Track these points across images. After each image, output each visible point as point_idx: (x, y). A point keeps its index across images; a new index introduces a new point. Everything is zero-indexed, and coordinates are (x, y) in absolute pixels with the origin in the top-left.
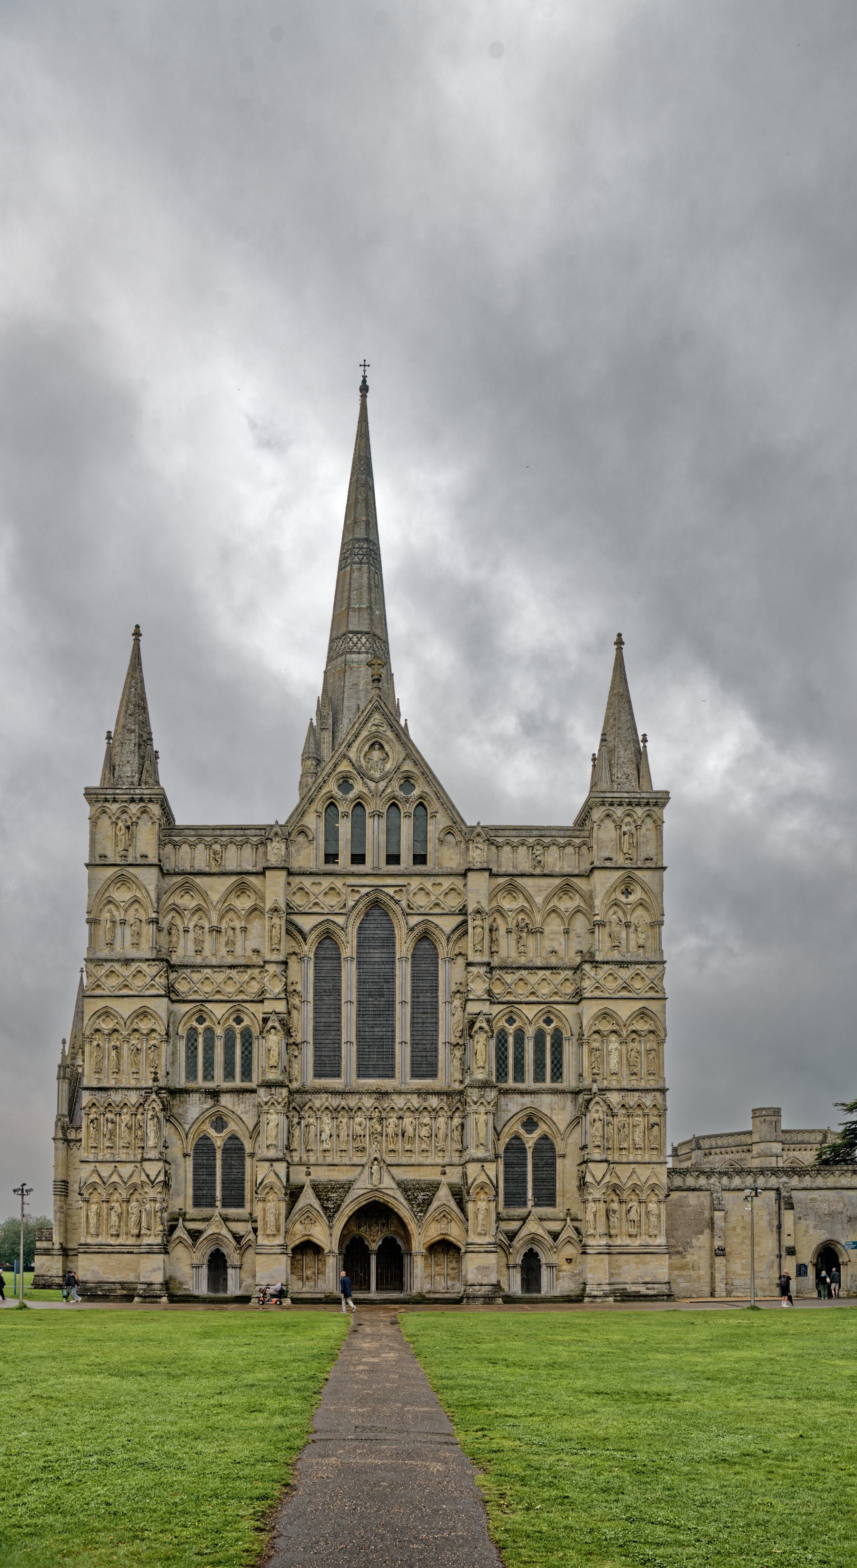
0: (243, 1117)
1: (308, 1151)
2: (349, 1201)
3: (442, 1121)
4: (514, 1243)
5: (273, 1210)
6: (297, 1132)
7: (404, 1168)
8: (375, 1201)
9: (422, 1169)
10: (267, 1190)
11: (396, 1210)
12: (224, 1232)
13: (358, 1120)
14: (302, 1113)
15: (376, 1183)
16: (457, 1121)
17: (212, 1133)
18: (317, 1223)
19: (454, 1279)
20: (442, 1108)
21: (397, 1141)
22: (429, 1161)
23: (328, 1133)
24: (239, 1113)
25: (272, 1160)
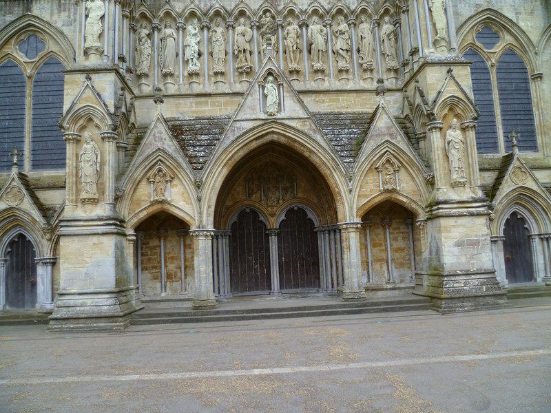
0: (66, 30)
1: (165, 76)
2: (228, 142)
3: (365, 27)
4: (495, 203)
5: (90, 156)
6: (146, 48)
7: (314, 96)
8: (272, 143)
9: (342, 97)
10: (81, 122)
11: (307, 154)
12: (27, 205)
13: (239, 29)
14: (156, 21)
15: (272, 109)
16: (387, 28)
17: (21, 57)
18: (176, 182)
19: (402, 265)
20: (364, 11)
21: (301, 59)
22: (350, 86)
23: (196, 48)
24: (59, 25)
25: (88, 72)
